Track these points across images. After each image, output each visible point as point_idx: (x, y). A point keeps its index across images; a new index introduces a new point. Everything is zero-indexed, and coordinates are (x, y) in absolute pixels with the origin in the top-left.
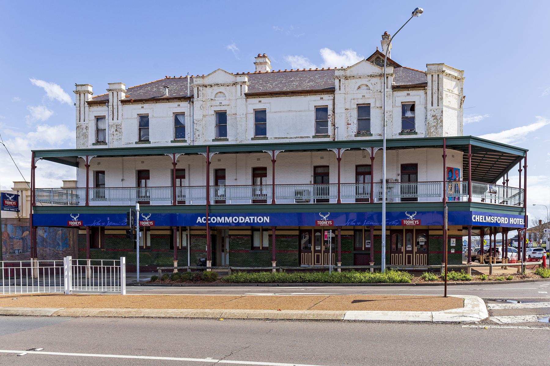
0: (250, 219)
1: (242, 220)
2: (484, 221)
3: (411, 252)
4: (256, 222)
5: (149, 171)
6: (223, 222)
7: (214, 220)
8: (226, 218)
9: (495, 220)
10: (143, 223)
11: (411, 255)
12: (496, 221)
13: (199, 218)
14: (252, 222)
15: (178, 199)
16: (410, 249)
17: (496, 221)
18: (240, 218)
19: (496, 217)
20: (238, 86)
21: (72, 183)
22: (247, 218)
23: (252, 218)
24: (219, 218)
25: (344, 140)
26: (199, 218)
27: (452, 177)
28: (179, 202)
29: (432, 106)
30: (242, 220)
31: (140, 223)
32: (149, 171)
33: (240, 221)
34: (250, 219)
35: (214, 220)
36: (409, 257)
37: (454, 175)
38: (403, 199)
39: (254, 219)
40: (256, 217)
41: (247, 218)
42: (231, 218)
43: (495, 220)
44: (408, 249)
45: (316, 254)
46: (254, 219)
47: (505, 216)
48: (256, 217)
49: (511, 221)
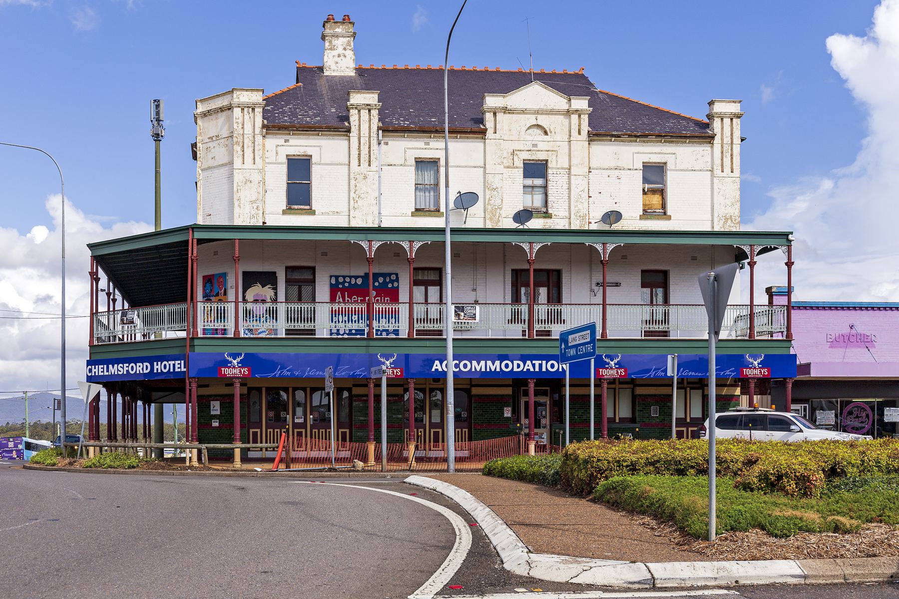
0: (534, 365)
1: (519, 366)
2: (106, 373)
3: (304, 425)
4: (544, 369)
5: (275, 273)
6: (483, 370)
7: (465, 366)
8: (489, 363)
9: (126, 369)
10: (606, 373)
11: (303, 431)
12: (128, 371)
13: (437, 362)
14: (537, 369)
15: (417, 326)
16: (438, 420)
17: (128, 371)
18: (516, 363)
19: (126, 365)
20: (575, 117)
21: (289, 292)
22: (529, 362)
23: (537, 363)
24: (474, 363)
25: (246, 223)
26: (437, 362)
27: (211, 291)
28: (539, 333)
29: (370, 165)
30: (519, 366)
31: (597, 372)
32: (275, 273)
33: (516, 369)
34: (534, 365)
35: (465, 366)
36: (436, 434)
37: (216, 287)
38: (288, 332)
39: (540, 365)
40: (544, 362)
41: (529, 362)
42: (497, 363)
43: (126, 369)
44: (296, 421)
45: (296, 431)
46: (540, 365)
47: (142, 360)
48: (544, 362)
49: (156, 367)
